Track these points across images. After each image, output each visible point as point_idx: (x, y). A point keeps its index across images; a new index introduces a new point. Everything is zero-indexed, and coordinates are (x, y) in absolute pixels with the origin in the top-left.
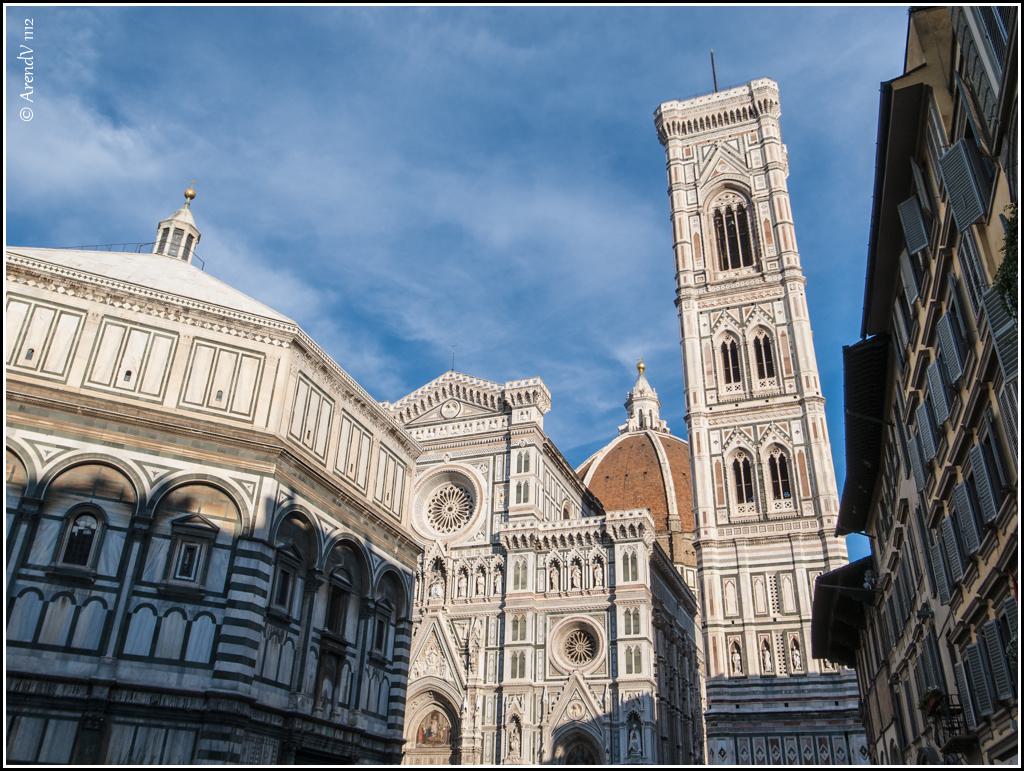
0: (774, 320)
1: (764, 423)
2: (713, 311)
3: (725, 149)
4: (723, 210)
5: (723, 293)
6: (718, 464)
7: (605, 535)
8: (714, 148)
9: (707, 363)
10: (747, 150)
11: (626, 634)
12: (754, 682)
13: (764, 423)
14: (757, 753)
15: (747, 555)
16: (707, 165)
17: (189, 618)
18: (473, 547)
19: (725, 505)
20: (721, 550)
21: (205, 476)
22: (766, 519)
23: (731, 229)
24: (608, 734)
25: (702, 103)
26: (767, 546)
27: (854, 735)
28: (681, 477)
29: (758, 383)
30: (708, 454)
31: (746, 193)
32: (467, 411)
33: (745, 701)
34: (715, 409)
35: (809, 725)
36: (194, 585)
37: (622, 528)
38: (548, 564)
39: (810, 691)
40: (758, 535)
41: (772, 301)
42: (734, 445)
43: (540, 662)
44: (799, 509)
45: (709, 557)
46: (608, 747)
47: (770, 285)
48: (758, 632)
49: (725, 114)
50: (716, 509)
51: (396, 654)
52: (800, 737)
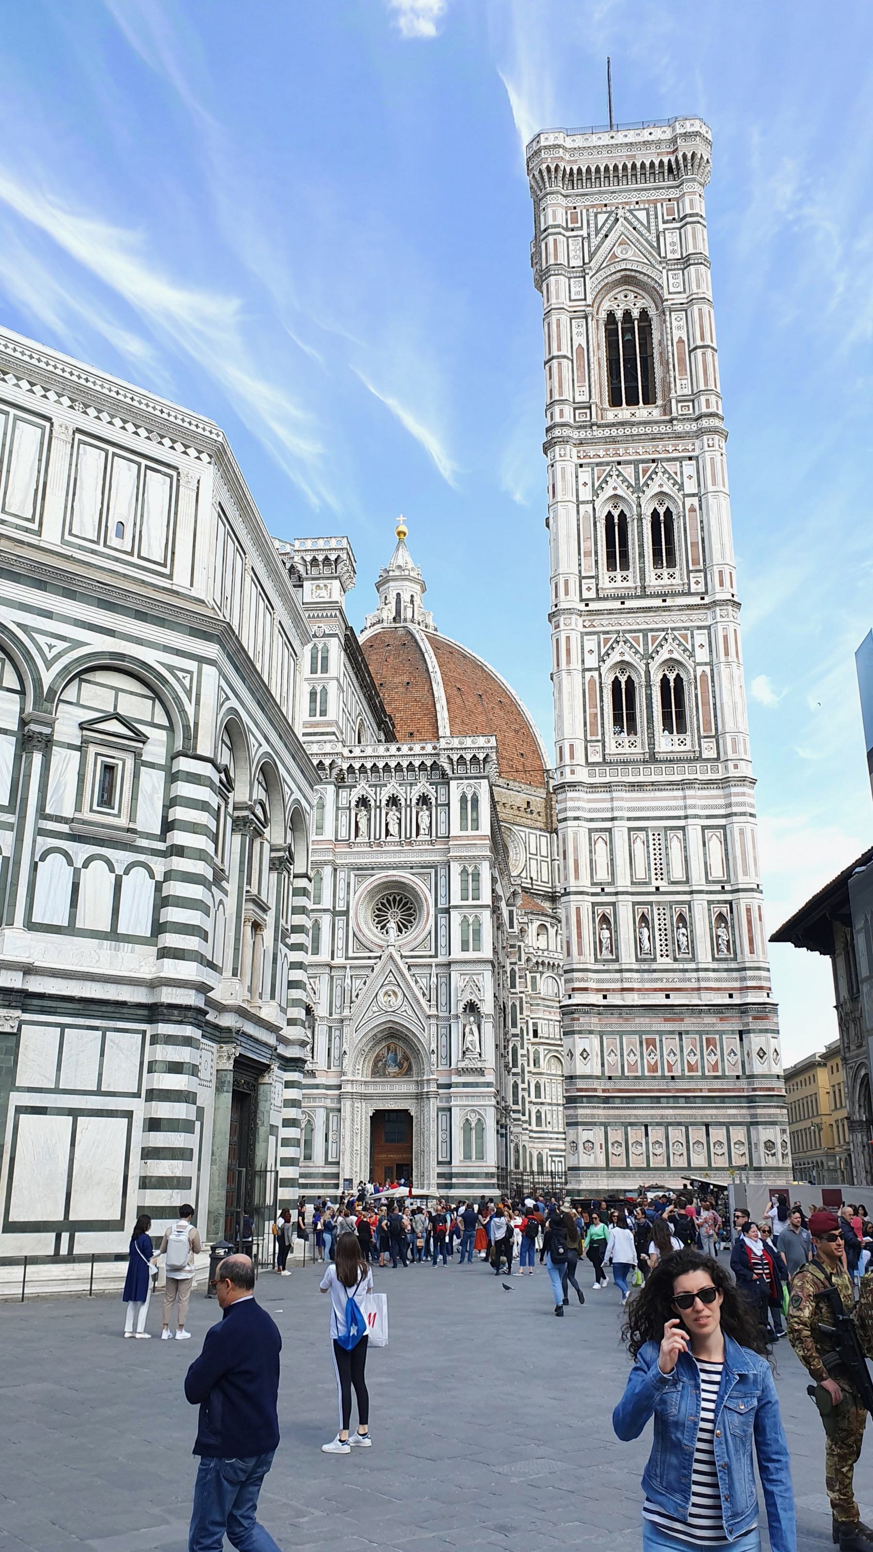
0: (681, 488)
1: (658, 630)
2: (598, 464)
3: (630, 223)
4: (619, 315)
5: (613, 440)
8: (612, 219)
10: (661, 229)
12: (627, 967)
13: (658, 630)
14: (629, 1055)
16: (602, 242)
17: (119, 871)
19: (599, 738)
21: (122, 656)
22: (653, 758)
23: (629, 345)
24: (434, 1029)
25: (601, 143)
26: (652, 794)
27: (752, 1035)
28: (456, 692)
29: (653, 574)
30: (580, 667)
31: (654, 292)
33: (614, 990)
34: (593, 606)
35: (694, 1020)
36: (123, 821)
38: (353, 803)
39: (698, 980)
40: (641, 779)
41: (680, 460)
42: (615, 657)
43: (340, 933)
44: (697, 748)
45: (577, 804)
46: (433, 1046)
47: (679, 437)
48: (634, 904)
49: (634, 166)
52: (684, 1037)
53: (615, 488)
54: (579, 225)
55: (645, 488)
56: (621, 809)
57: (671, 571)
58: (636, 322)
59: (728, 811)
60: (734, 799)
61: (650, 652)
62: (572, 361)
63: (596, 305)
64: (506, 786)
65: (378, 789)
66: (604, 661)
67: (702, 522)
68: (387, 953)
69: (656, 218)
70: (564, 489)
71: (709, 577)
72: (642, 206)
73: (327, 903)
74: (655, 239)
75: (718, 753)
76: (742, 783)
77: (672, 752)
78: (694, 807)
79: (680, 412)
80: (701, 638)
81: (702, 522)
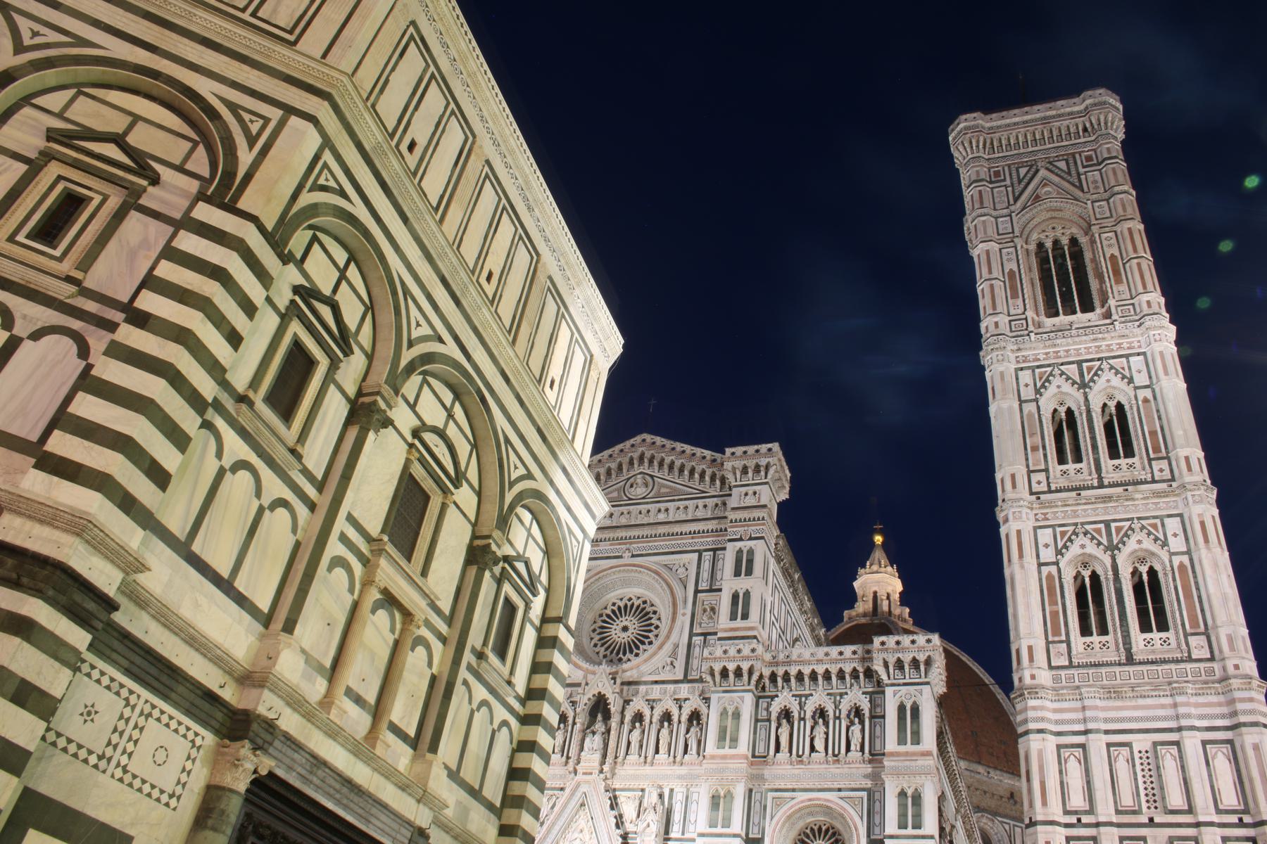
0: (1131, 381)
2: (1038, 367)
6: (1050, 576)
7: (869, 673)
8: (1033, 170)
11: (899, 828)
15: (1102, 715)
17: (20, 329)
18: (656, 682)
19: (1063, 638)
22: (1130, 660)
26: (1133, 703)
32: (663, 490)
37: (900, 665)
38: (774, 716)
41: (1127, 356)
44: (1184, 646)
45: (1040, 714)
50: (1048, 643)
53: (1059, 387)
54: (1002, 178)
55: (1091, 384)
56: (1095, 719)
57: (1130, 461)
58: (1066, 248)
61: (1115, 542)
62: (1004, 282)
63: (1024, 236)
64: (986, 774)
65: (803, 699)
66: (1062, 555)
67: (1158, 411)
69: (1075, 163)
70: (1004, 390)
71: (1174, 463)
72: (1061, 158)
74: (1076, 181)
75: (1212, 652)
77: (1153, 652)
78: (1189, 716)
79: (1120, 315)
80: (1173, 525)
81: (1158, 411)
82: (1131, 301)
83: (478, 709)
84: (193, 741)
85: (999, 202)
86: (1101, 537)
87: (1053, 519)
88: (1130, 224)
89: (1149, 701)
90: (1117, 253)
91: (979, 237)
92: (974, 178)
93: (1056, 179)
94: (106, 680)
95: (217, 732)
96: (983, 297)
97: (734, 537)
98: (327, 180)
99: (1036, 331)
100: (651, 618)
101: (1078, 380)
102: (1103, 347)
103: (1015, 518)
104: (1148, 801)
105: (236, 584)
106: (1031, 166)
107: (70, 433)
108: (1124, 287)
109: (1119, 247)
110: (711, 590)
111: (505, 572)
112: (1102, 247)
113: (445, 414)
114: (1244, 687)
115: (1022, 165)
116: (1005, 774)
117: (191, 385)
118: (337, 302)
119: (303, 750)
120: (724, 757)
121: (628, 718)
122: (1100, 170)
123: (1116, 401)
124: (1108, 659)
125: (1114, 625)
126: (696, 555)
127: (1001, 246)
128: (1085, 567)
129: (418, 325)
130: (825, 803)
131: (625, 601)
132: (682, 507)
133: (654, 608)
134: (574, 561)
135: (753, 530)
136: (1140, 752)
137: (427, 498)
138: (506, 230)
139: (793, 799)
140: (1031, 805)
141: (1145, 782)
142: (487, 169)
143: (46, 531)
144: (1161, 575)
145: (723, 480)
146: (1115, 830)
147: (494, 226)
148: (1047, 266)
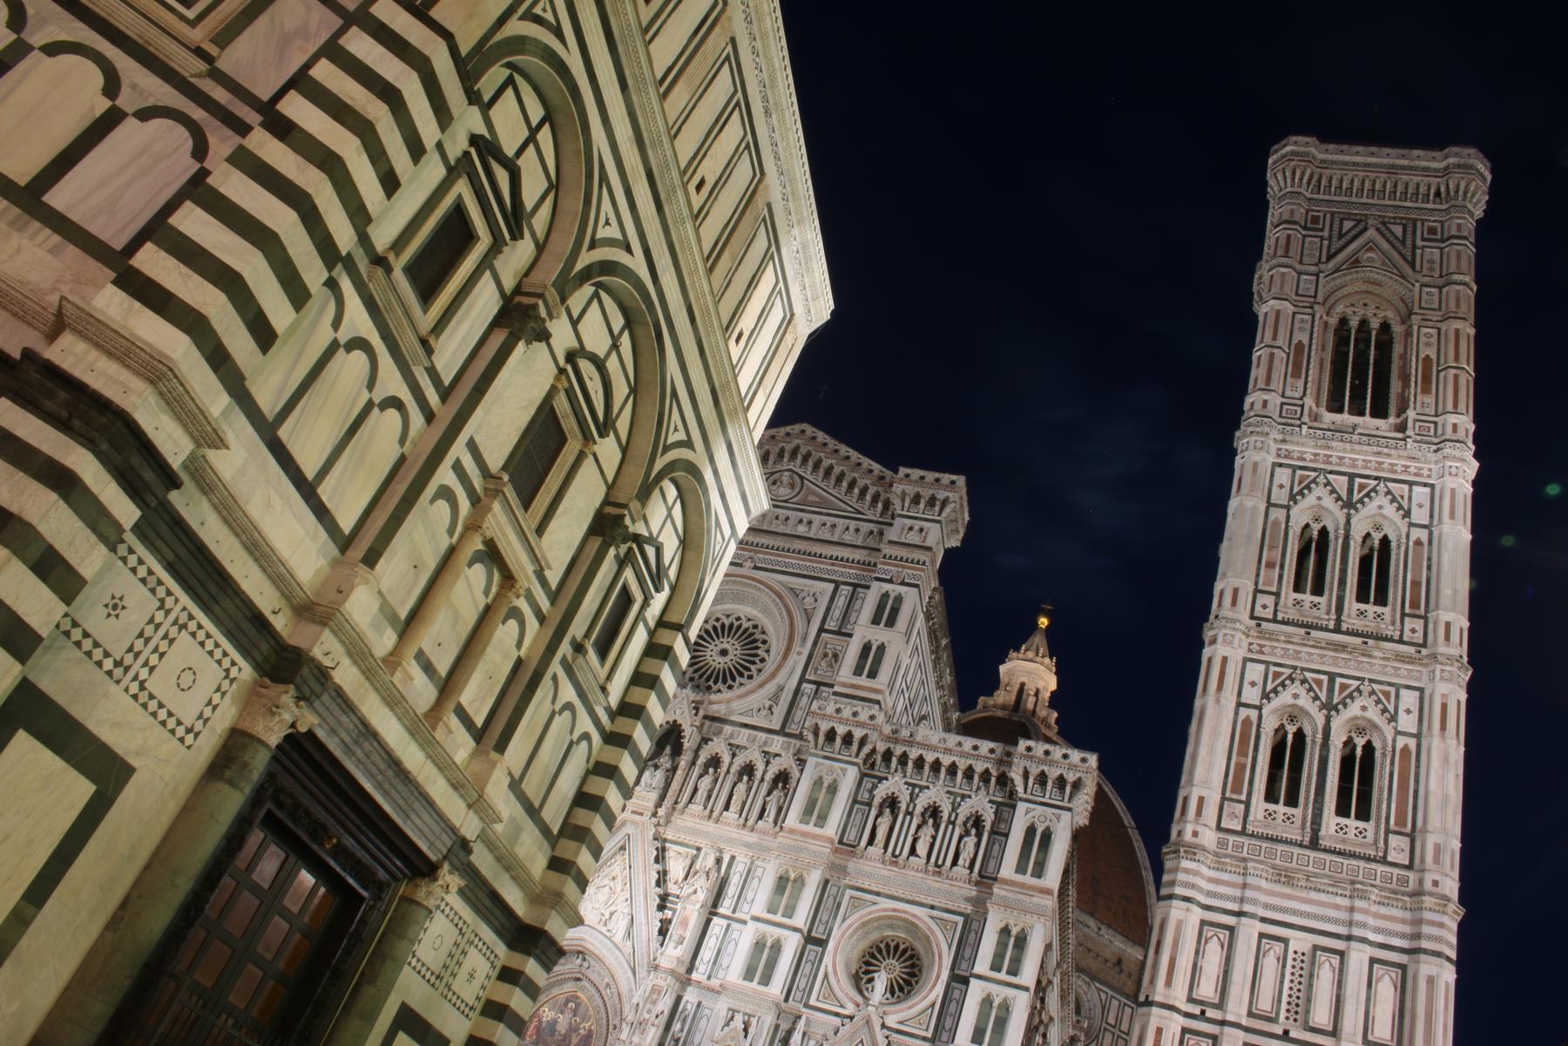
0: (1407, 514)
2: (1301, 468)
4: (1354, 323)
6: (1247, 722)
7: (1003, 780)
8: (1361, 227)
9: (1272, 548)
17: (125, 101)
18: (746, 726)
19: (1243, 797)
20: (1213, 874)
22: (1314, 844)
26: (1304, 894)
32: (811, 498)
37: (1042, 779)
41: (1411, 484)
44: (1381, 844)
45: (1191, 879)
50: (1224, 798)
51: (630, 699)
53: (1319, 498)
54: (1320, 226)
55: (1359, 506)
56: (1255, 902)
57: (1379, 609)
58: (1374, 333)
59: (1415, 944)
60: (1426, 929)
61: (1335, 702)
62: (1288, 354)
63: (1327, 305)
64: (1096, 930)
66: (1269, 700)
67: (1429, 559)
68: (863, 1013)
70: (1253, 485)
71: (1431, 626)
72: (1398, 221)
73: (801, 918)
76: (1441, 909)
77: (1344, 841)
78: (1364, 925)
79: (1417, 431)
80: (1409, 699)
81: (1429, 559)
82: (1435, 419)
83: (561, 712)
84: (227, 671)
85: (1308, 255)
86: (1321, 691)
87: (1270, 654)
88: (1458, 325)
89: (1323, 897)
90: (1433, 356)
91: (1273, 290)
92: (1286, 217)
93: (1385, 245)
94: (142, 572)
95: (257, 666)
96: (1258, 365)
97: (884, 576)
98: (544, 10)
99: (1310, 424)
100: (758, 648)
101: (1344, 497)
102: (1386, 466)
103: (1224, 641)
104: (1288, 1011)
105: (320, 491)
106: (1359, 222)
107: (166, 251)
108: (1430, 400)
109: (1439, 350)
110: (839, 633)
111: (632, 553)
112: (1418, 343)
113: (610, 342)
114: (1437, 908)
115: (1348, 217)
116: (1117, 935)
117: (325, 227)
118: (519, 169)
119: (355, 713)
120: (805, 835)
121: (702, 760)
122: (1442, 249)
123: (1383, 534)
124: (1289, 836)
125: (1307, 798)
126: (831, 586)
127: (1296, 310)
128: (1292, 721)
129: (607, 223)
130: (910, 918)
131: (732, 619)
132: (829, 524)
133: (765, 637)
134: (714, 560)
135: (908, 573)
136: (1295, 952)
137: (563, 440)
138: (734, 131)
139: (874, 903)
140: (1153, 981)
141: (1291, 989)
142: (729, 48)
143: (112, 368)
144: (1378, 754)
145: (887, 504)
146: (1241, 1034)
147: (720, 123)
148: (1345, 349)
